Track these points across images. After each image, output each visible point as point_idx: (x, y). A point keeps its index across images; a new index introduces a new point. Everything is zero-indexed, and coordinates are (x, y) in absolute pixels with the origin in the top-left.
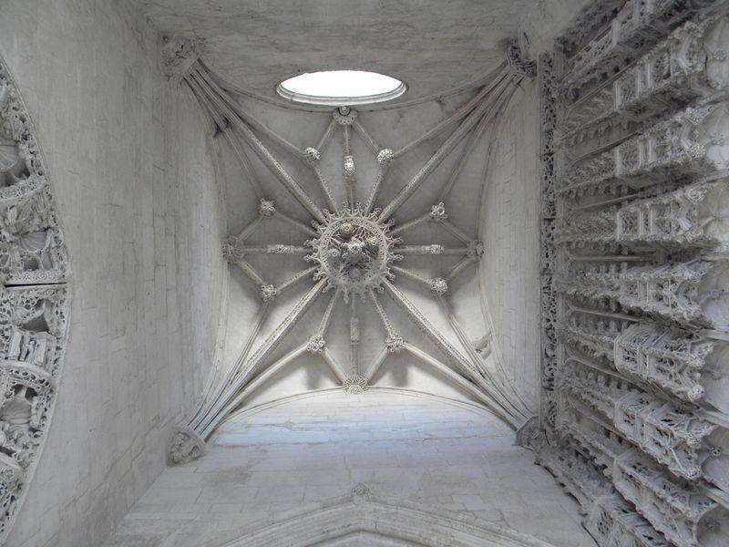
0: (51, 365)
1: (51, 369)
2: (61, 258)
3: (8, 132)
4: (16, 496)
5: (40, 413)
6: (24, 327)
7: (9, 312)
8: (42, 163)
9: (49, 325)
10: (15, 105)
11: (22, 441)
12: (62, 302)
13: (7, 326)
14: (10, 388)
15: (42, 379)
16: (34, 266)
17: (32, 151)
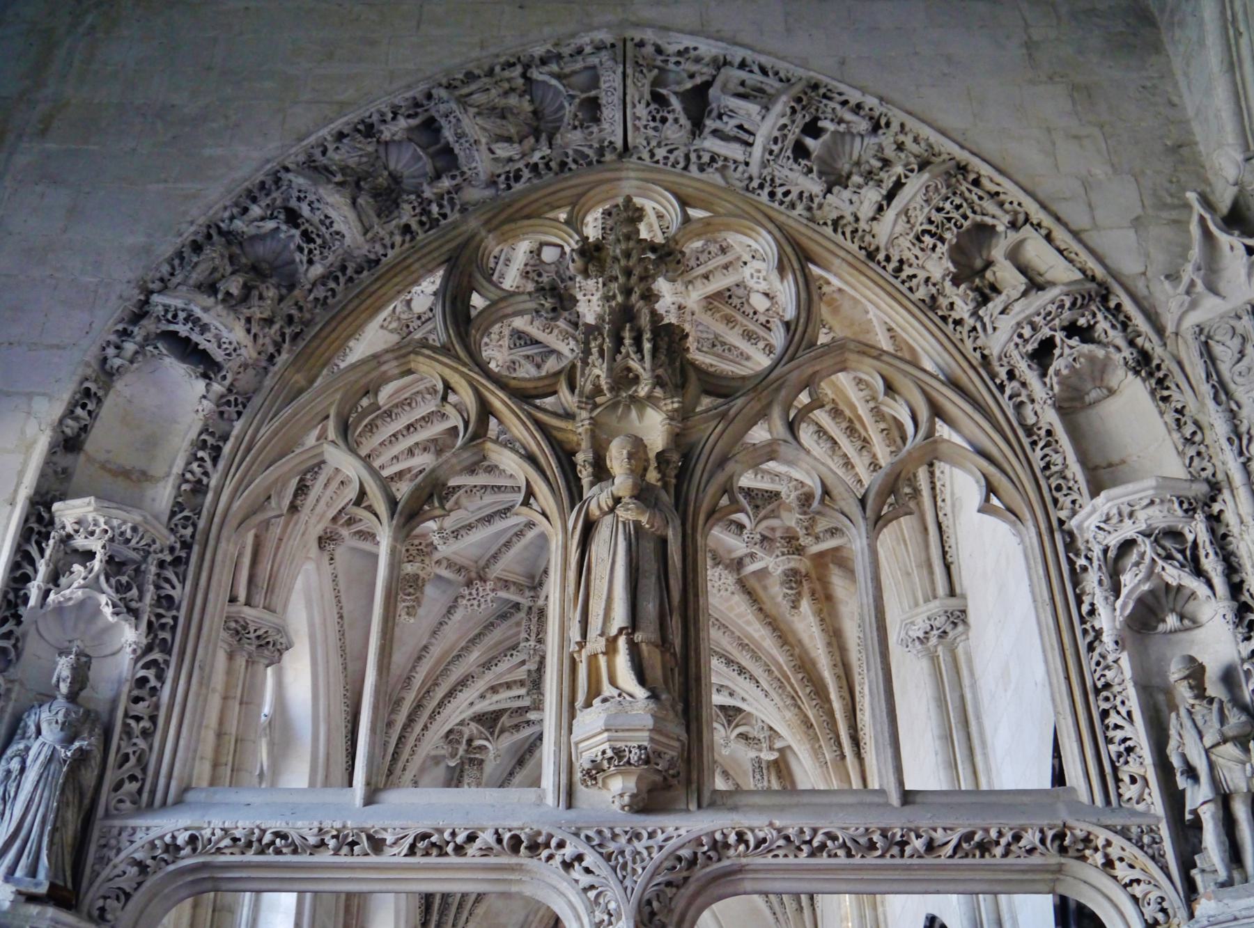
0: (771, 84)
1: (778, 85)
2: (580, 51)
3: (364, 159)
4: (972, 177)
5: (848, 116)
6: (697, 127)
7: (670, 151)
8: (409, 94)
9: (698, 80)
10: (317, 152)
11: (890, 152)
12: (659, 51)
13: (693, 157)
14: (795, 166)
15: (788, 111)
16: (592, 108)
17: (390, 115)
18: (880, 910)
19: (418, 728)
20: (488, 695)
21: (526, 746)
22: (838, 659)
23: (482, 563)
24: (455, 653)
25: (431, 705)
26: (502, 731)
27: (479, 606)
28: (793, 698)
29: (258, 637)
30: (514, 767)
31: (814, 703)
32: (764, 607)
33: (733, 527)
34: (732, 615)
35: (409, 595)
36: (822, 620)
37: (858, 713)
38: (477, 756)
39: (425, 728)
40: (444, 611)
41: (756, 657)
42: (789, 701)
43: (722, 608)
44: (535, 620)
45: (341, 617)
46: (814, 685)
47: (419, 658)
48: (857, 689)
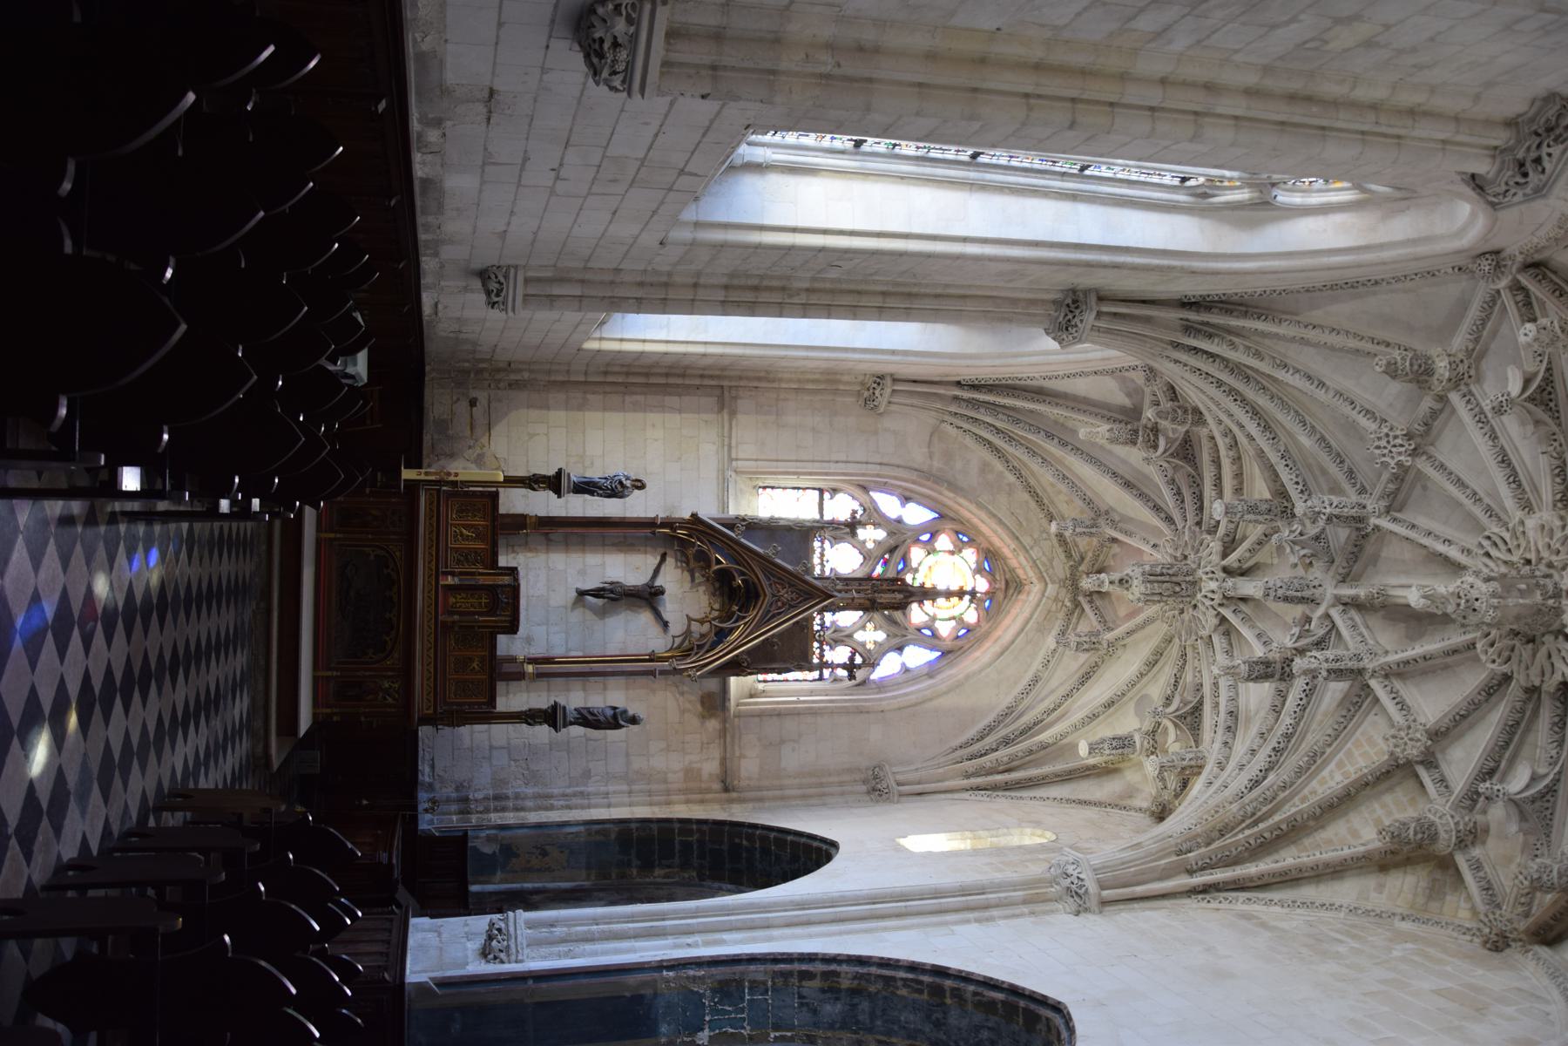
18: (1025, 909)
19: (1224, 377)
20: (1231, 453)
21: (1145, 490)
22: (1306, 874)
23: (1431, 450)
24: (1307, 417)
25: (1249, 393)
26: (1176, 468)
27: (1378, 447)
28: (1254, 814)
29: (1538, 161)
30: (1122, 478)
31: (1252, 842)
32: (1368, 788)
33: (1492, 764)
34: (1349, 745)
35: (1411, 365)
36: (1358, 859)
37: (1243, 895)
38: (1141, 438)
39: (1220, 384)
40: (1367, 407)
41: (1300, 772)
42: (1249, 809)
43: (1358, 733)
44: (1353, 512)
45: (1376, 283)
46: (1269, 843)
47: (1309, 378)
48: (1276, 895)
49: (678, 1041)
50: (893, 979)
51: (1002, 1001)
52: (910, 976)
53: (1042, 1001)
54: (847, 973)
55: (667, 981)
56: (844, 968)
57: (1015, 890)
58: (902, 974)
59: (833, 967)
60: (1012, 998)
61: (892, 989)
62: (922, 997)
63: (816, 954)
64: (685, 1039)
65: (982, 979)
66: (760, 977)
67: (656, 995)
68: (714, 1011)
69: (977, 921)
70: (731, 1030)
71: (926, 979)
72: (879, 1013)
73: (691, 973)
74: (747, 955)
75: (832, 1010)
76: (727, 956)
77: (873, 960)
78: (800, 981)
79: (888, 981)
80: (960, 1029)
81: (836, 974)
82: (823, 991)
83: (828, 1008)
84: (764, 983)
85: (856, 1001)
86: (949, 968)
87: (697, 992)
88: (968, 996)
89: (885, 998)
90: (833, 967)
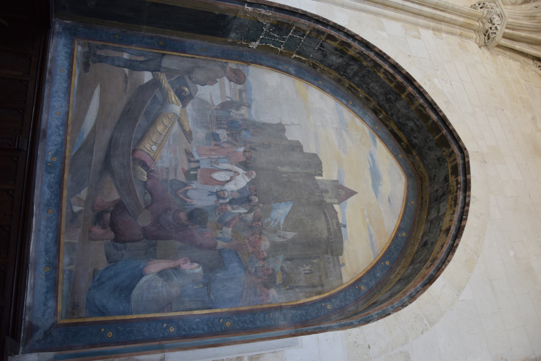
18: (458, 31)
49: (239, 43)
50: (381, 67)
51: (433, 121)
52: (391, 71)
53: (457, 140)
54: (356, 48)
55: (246, 12)
56: (356, 44)
57: (460, 16)
58: (387, 67)
59: (350, 41)
60: (440, 123)
61: (376, 70)
62: (390, 84)
63: (344, 28)
64: (243, 43)
65: (430, 101)
66: (304, 27)
67: (235, 18)
68: (267, 34)
69: (434, 29)
70: (272, 46)
71: (399, 78)
72: (360, 75)
73: (263, 12)
74: (302, 11)
75: (335, 59)
76: (290, 7)
77: (375, 49)
78: (327, 38)
79: (377, 65)
80: (399, 111)
81: (350, 46)
82: (336, 49)
83: (334, 58)
84: (304, 31)
85: (352, 63)
86: (415, 81)
87: (262, 23)
88: (417, 103)
89: (369, 72)
90: (350, 41)
